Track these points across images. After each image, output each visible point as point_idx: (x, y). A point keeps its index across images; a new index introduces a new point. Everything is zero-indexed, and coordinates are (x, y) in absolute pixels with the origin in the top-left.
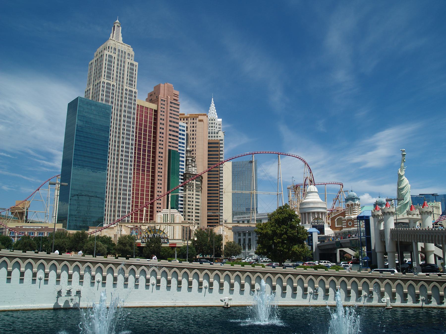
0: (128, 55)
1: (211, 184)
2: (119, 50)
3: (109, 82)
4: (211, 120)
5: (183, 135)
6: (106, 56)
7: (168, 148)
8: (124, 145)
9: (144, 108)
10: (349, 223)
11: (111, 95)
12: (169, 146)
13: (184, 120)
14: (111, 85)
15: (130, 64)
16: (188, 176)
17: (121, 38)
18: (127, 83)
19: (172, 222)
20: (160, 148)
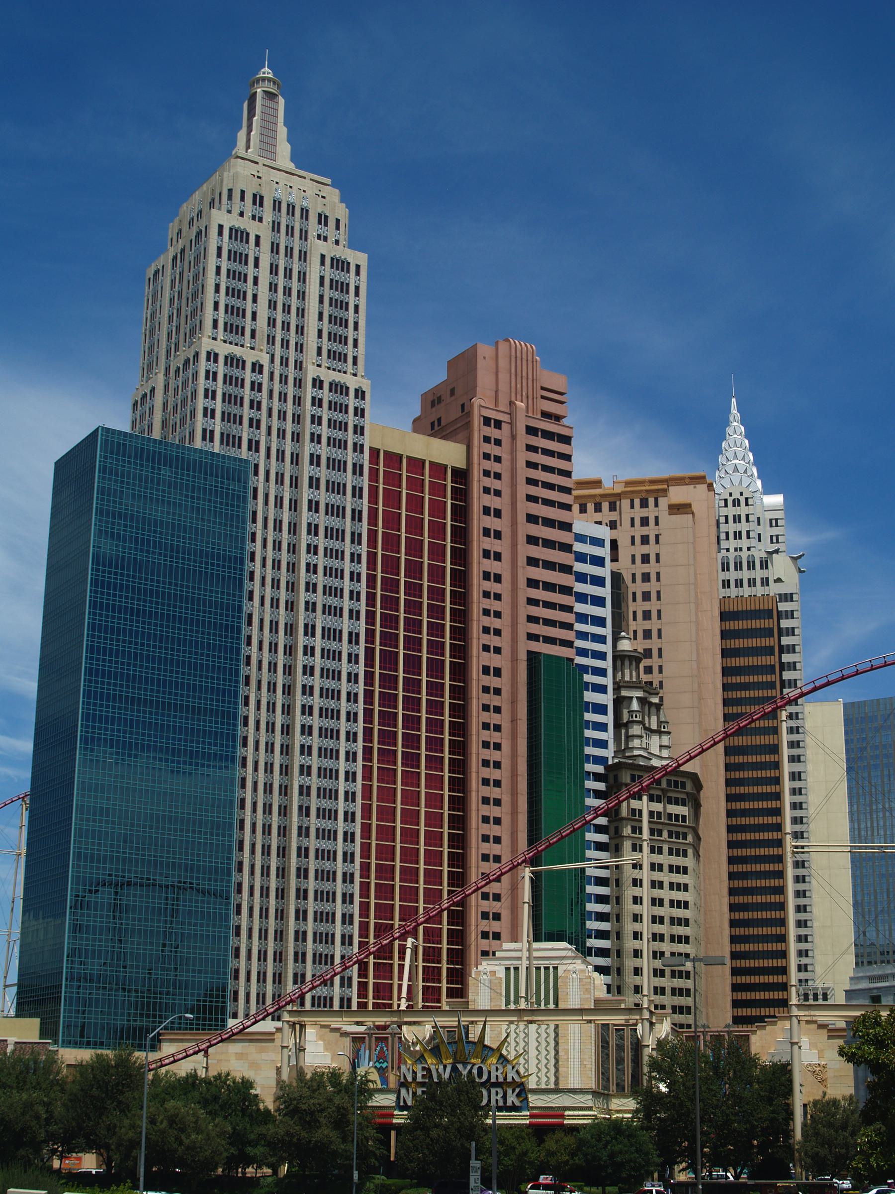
0: (320, 223)
1: (744, 813)
2: (277, 205)
3: (237, 351)
4: (730, 503)
5: (598, 581)
6: (220, 233)
7: (525, 646)
8: (318, 642)
9: (404, 461)
11: (247, 413)
12: (532, 637)
13: (598, 508)
14: (249, 367)
15: (328, 261)
16: (626, 777)
17: (284, 149)
18: (319, 353)
19: (547, 1003)
20: (486, 648)
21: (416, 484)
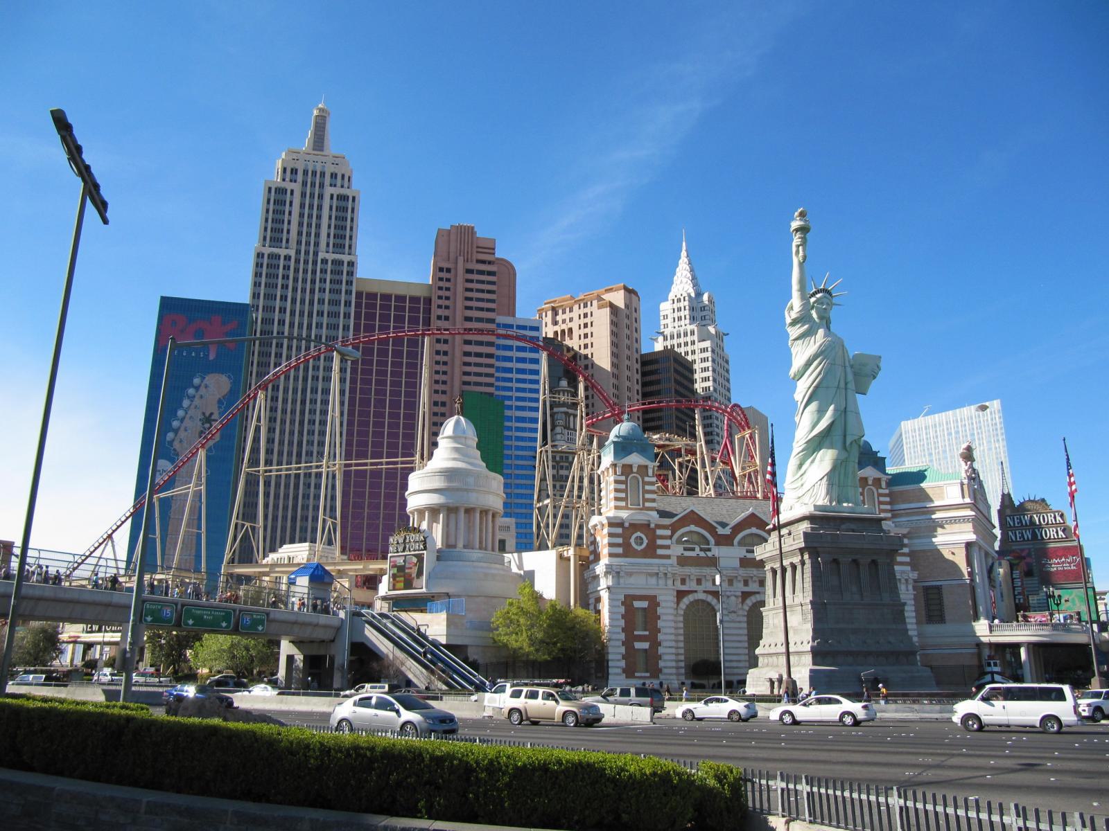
10: (641, 544)
14: (346, 264)
15: (335, 197)
21: (386, 307)
